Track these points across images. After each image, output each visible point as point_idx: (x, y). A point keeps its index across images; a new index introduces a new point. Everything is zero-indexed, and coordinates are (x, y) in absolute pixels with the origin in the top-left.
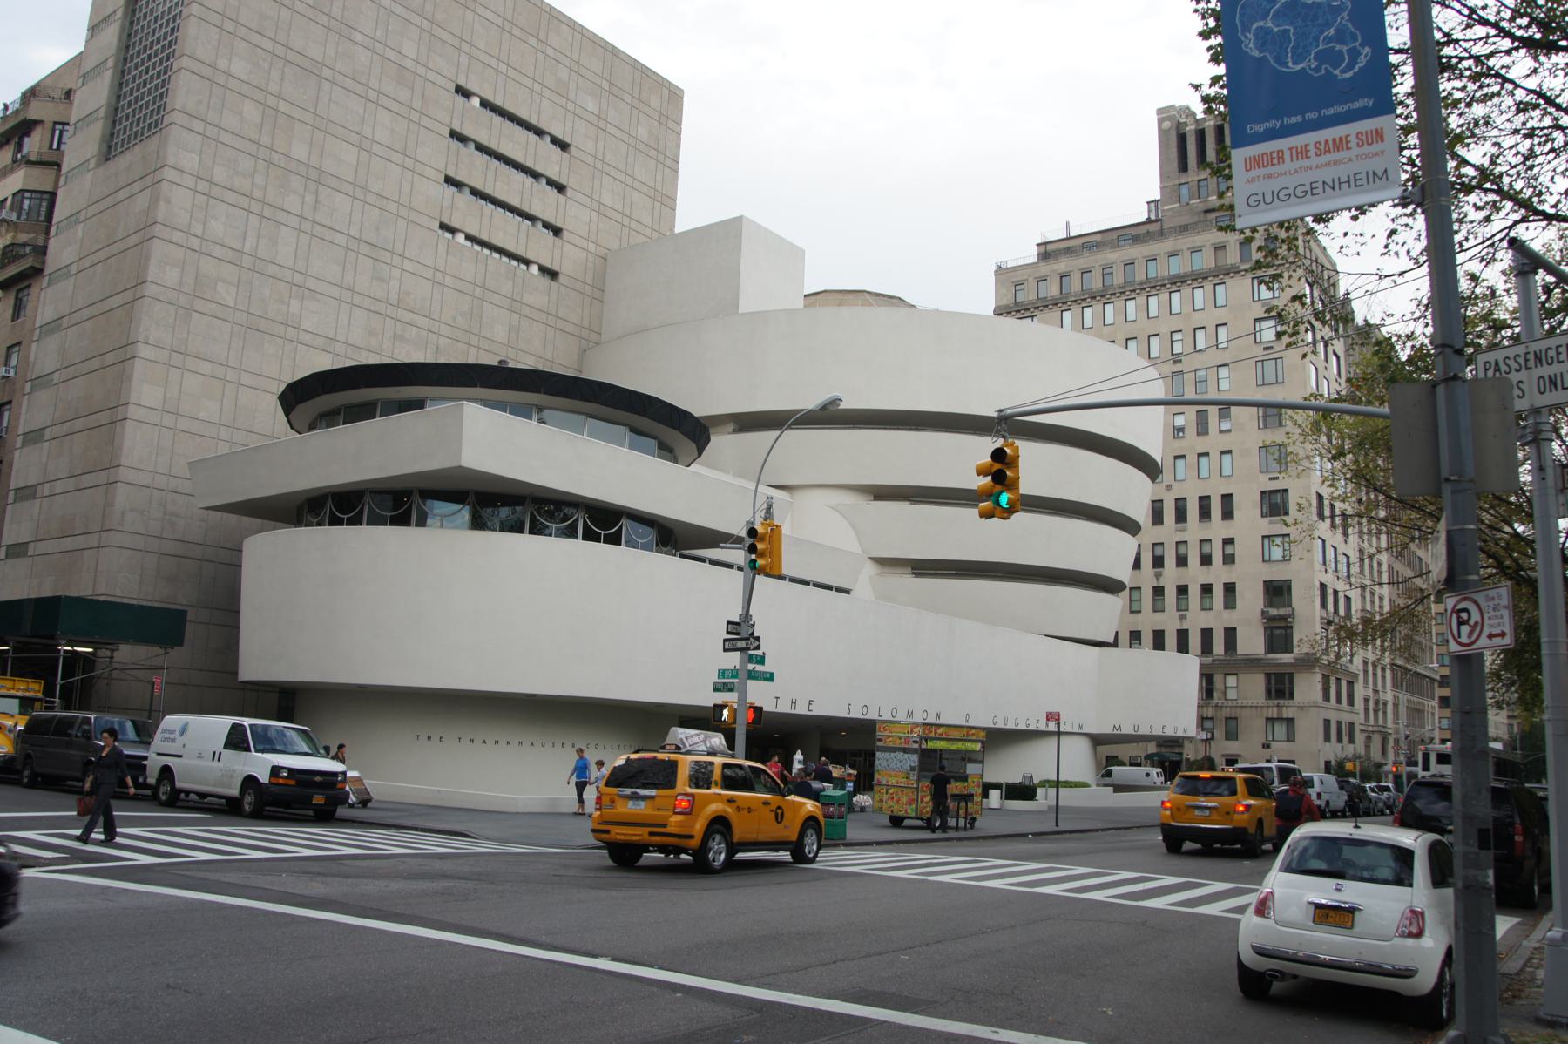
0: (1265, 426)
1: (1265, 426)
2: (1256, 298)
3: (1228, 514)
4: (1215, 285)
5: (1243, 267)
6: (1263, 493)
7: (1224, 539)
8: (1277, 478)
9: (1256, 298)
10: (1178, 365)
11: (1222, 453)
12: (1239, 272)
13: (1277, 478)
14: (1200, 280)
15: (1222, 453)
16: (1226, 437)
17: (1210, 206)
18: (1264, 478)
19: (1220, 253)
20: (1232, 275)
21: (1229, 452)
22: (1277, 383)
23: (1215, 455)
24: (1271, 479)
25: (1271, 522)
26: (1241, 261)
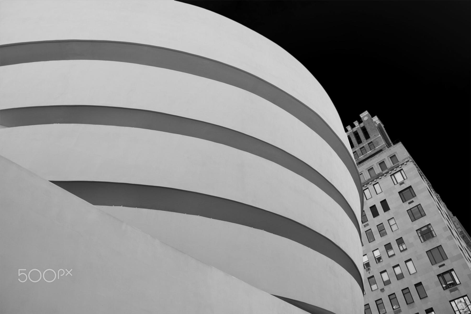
0: (425, 240)
1: (425, 240)
2: (396, 183)
3: (423, 296)
4: (374, 185)
5: (384, 172)
6: (438, 276)
7: (426, 310)
8: (444, 265)
9: (396, 183)
10: (367, 227)
11: (406, 262)
12: (383, 175)
13: (444, 265)
14: (365, 186)
15: (406, 262)
16: (405, 253)
17: (360, 160)
18: (436, 267)
19: (371, 171)
20: (380, 178)
21: (410, 260)
22: (422, 216)
23: (402, 264)
24: (440, 266)
25: (451, 291)
26: (382, 171)
